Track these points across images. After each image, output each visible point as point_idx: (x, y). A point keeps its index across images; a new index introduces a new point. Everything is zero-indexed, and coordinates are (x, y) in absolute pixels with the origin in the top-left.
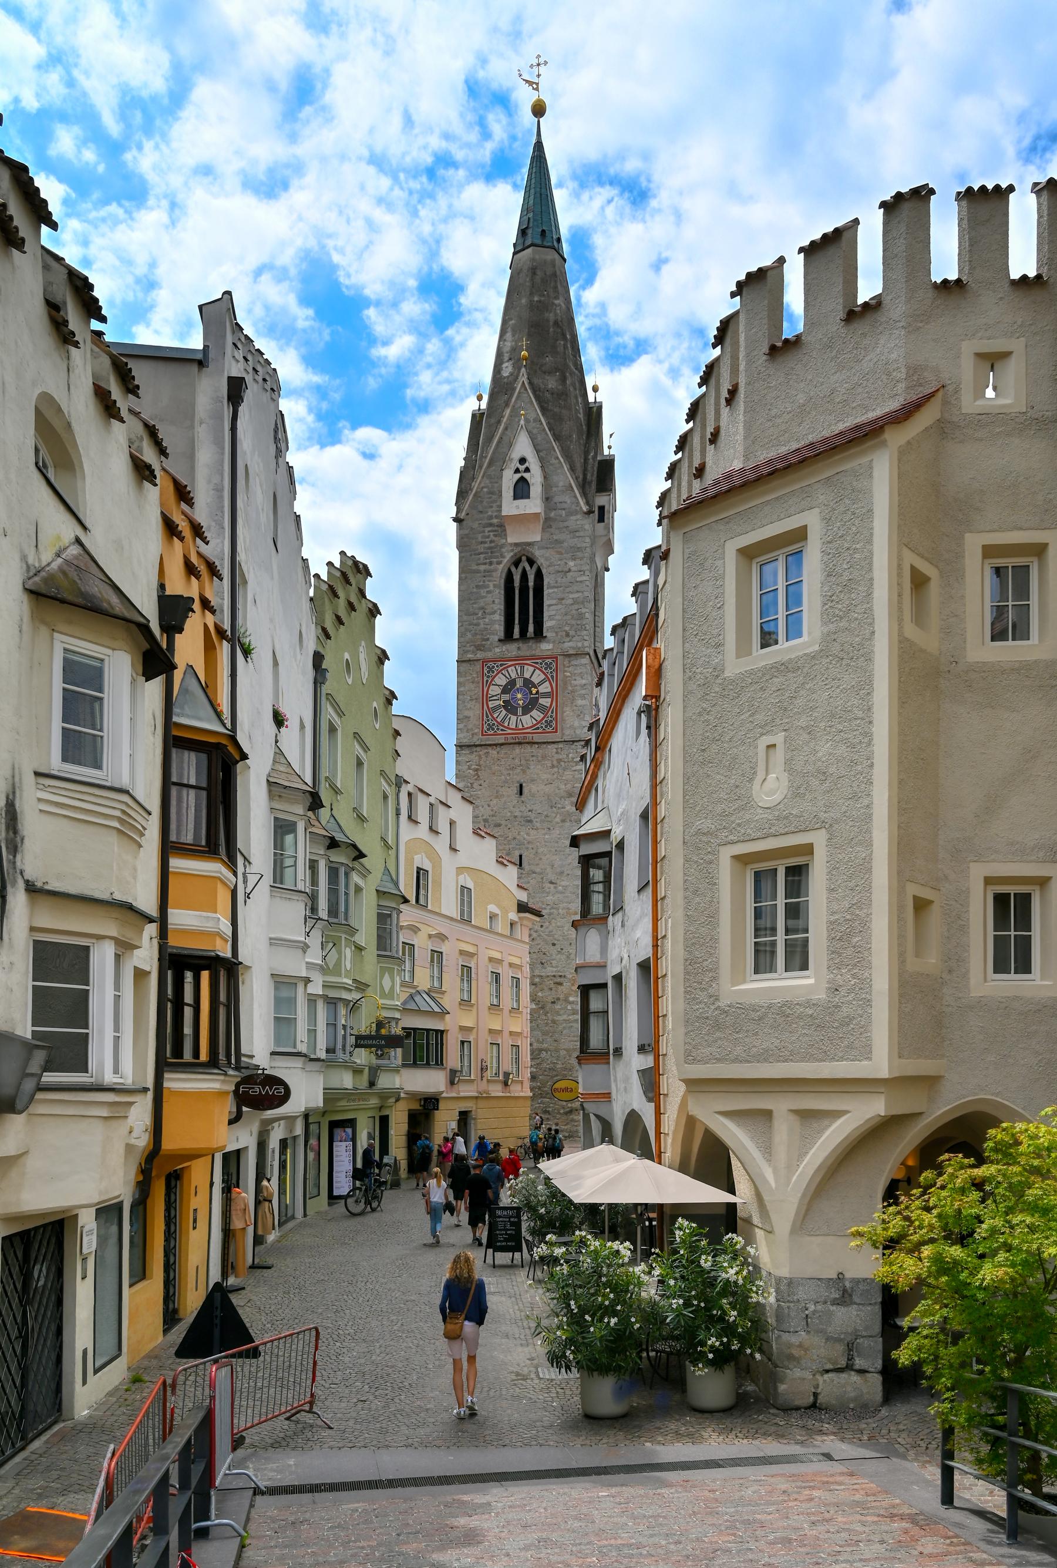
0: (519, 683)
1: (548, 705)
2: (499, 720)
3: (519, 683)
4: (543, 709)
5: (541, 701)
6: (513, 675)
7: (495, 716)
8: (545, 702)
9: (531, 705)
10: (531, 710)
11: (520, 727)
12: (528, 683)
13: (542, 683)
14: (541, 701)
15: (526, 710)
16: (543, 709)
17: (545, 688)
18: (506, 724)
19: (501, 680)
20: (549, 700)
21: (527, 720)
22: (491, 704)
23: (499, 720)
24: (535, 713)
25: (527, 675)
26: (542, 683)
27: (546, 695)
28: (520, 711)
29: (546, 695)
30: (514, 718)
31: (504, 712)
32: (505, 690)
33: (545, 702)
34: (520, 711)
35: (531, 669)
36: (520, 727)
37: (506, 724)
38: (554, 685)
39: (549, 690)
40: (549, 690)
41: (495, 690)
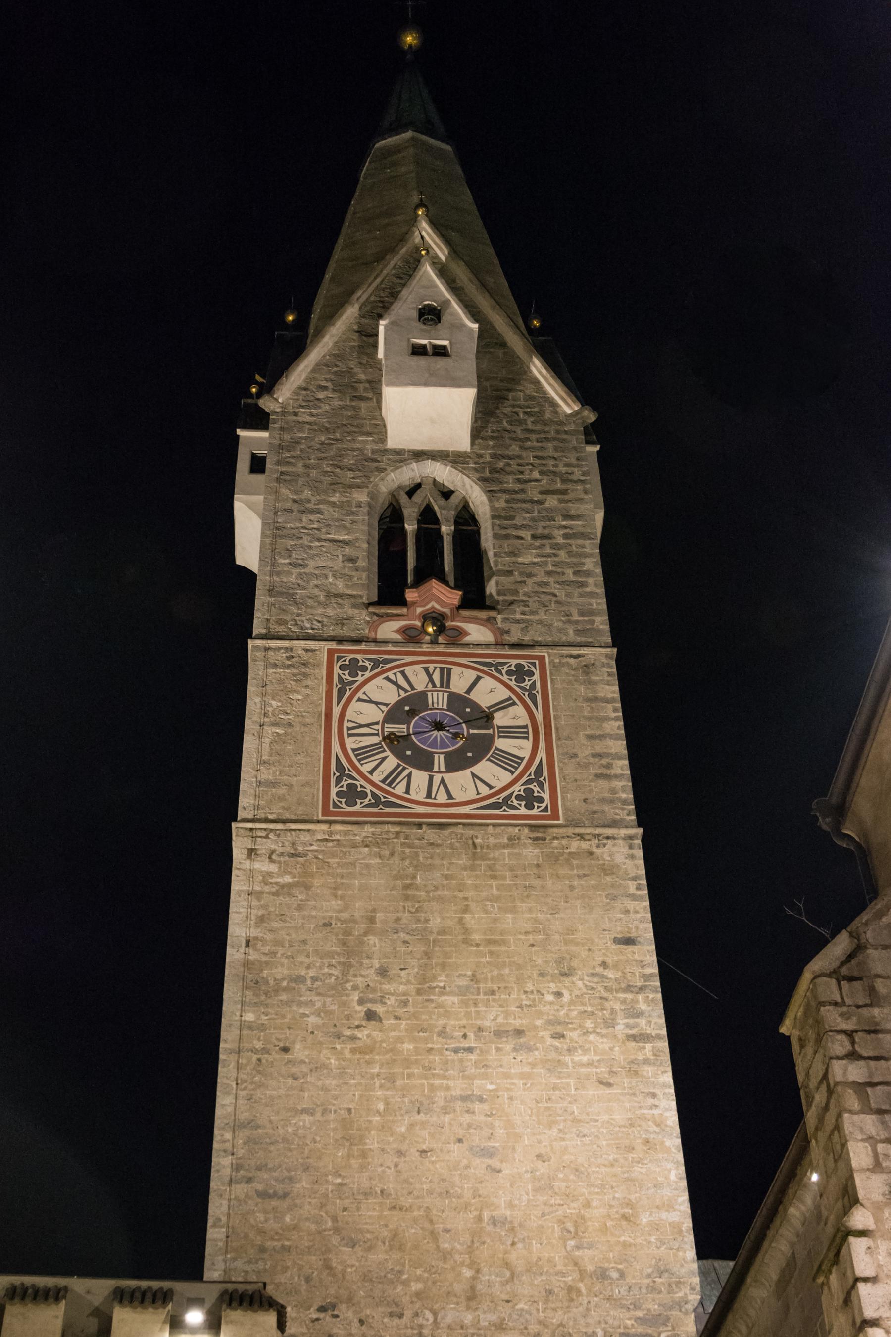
0: (439, 700)
1: (526, 754)
2: (377, 778)
3: (439, 700)
4: (508, 761)
6: (420, 682)
7: (366, 768)
12: (458, 702)
14: (501, 743)
15: (456, 763)
16: (508, 761)
17: (516, 716)
20: (528, 745)
21: (461, 784)
22: (351, 743)
23: (377, 778)
24: (484, 768)
28: (439, 761)
30: (420, 777)
31: (392, 761)
32: (394, 714)
34: (439, 761)
35: (472, 675)
36: (442, 798)
37: (400, 790)
40: (524, 720)
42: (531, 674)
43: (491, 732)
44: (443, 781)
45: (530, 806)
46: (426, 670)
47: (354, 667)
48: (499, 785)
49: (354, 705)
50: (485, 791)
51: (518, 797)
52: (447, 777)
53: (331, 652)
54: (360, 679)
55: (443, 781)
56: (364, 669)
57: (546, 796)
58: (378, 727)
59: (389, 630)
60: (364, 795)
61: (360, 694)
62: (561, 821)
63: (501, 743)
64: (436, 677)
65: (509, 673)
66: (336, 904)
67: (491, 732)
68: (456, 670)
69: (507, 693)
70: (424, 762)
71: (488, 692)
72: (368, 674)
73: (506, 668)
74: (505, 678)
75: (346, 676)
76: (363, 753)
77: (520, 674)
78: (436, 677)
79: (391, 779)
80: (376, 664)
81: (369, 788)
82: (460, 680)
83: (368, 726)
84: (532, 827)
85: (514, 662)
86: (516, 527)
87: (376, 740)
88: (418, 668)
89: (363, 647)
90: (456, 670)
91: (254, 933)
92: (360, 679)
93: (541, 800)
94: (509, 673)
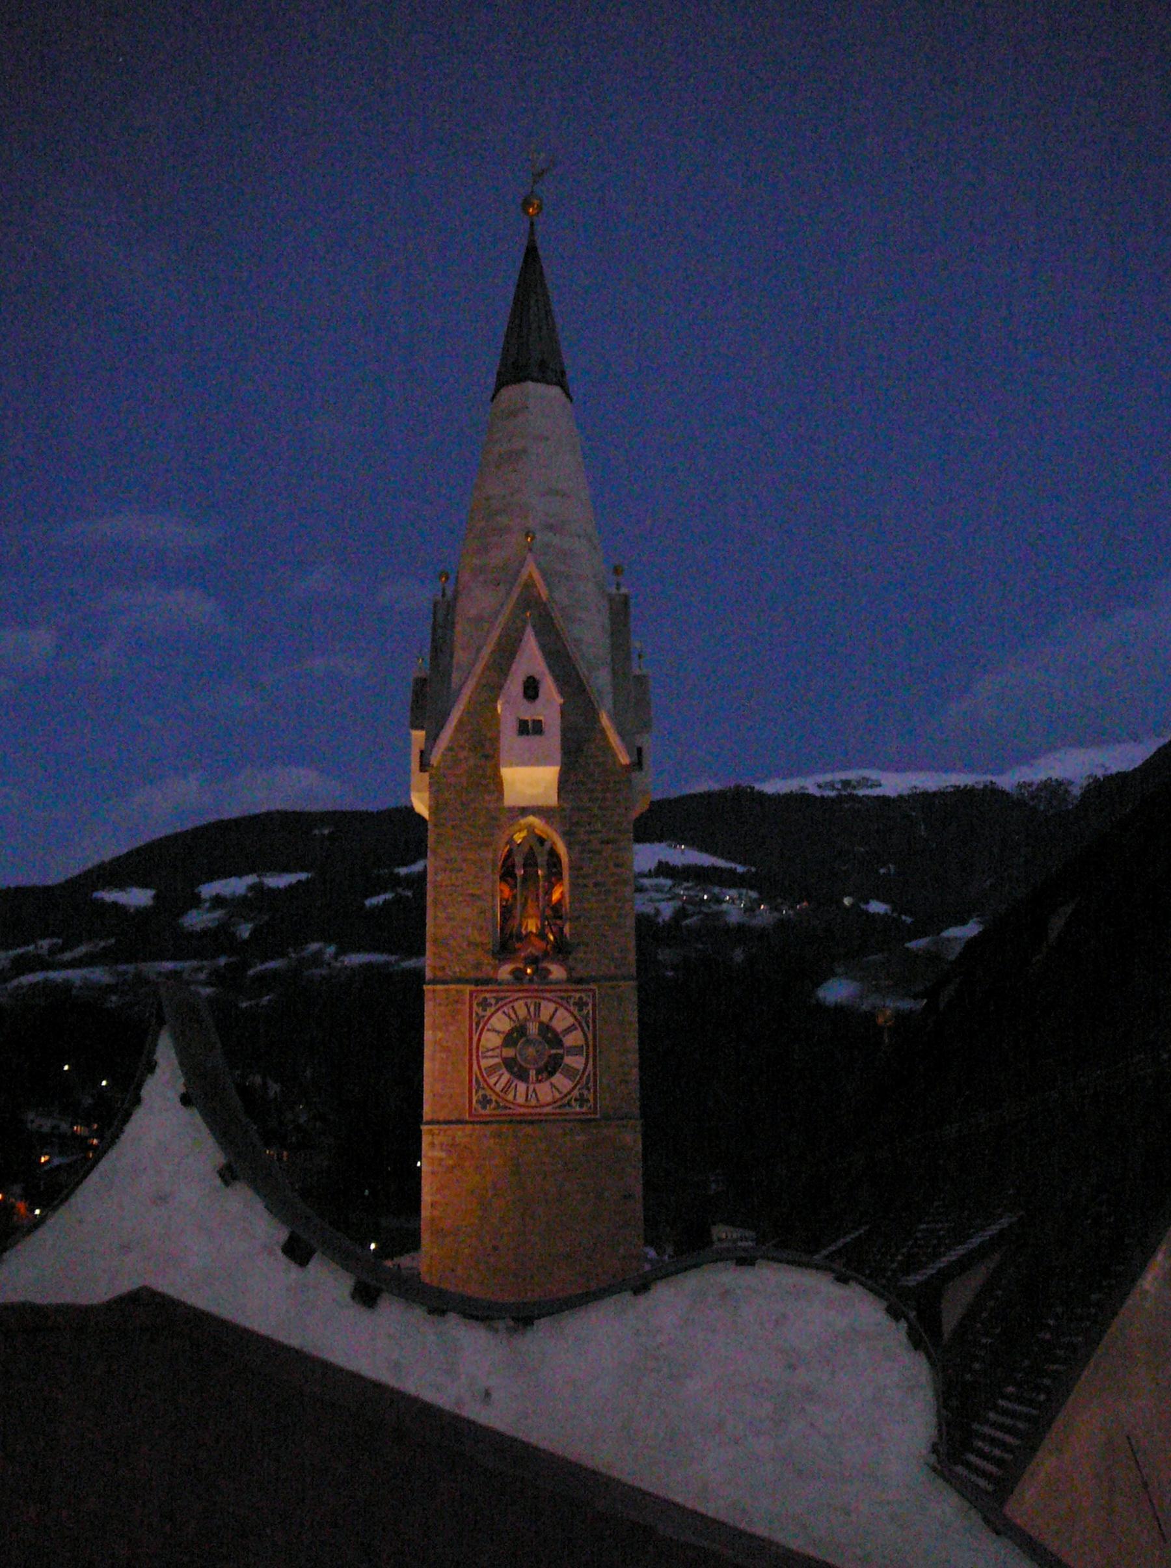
0: (533, 1029)
1: (581, 1067)
3: (533, 1029)
4: (570, 1073)
5: (568, 1060)
7: (492, 1081)
8: (575, 1062)
9: (552, 1067)
10: (551, 1074)
11: (533, 1102)
12: (545, 1028)
13: (569, 1030)
16: (570, 1073)
18: (510, 1097)
19: (501, 1022)
21: (545, 1092)
22: (485, 1063)
23: (498, 1088)
24: (560, 1080)
25: (544, 1017)
26: (569, 1030)
27: (575, 1051)
28: (532, 1073)
29: (575, 1051)
30: (522, 1087)
31: (506, 1076)
32: (510, 1039)
33: (575, 1062)
34: (532, 1073)
35: (552, 1006)
37: (510, 1097)
38: (590, 1037)
39: (581, 1042)
40: (581, 1042)
41: (491, 1040)
42: (586, 1004)
43: (560, 1051)
44: (534, 1090)
45: (581, 1106)
46: (526, 1004)
47: (484, 1004)
48: (565, 1091)
49: (486, 1034)
50: (558, 1095)
51: (576, 1100)
52: (538, 1086)
53: (471, 994)
54: (488, 1013)
55: (534, 1090)
56: (491, 1005)
57: (591, 1097)
58: (498, 1051)
59: (505, 972)
60: (490, 1102)
61: (488, 1026)
62: (598, 1116)
63: (568, 1060)
64: (532, 1009)
65: (575, 1004)
66: (478, 1178)
67: (560, 1051)
68: (544, 1003)
69: (571, 1020)
70: (522, 1075)
71: (562, 1020)
72: (493, 1009)
73: (572, 1001)
74: (572, 1008)
75: (480, 1011)
76: (492, 1070)
77: (581, 1004)
78: (532, 1009)
79: (505, 1090)
80: (498, 1000)
81: (494, 1098)
82: (547, 1009)
83: (493, 1050)
84: (580, 1121)
85: (578, 995)
86: (584, 877)
87: (498, 1060)
88: (521, 1002)
89: (490, 987)
90: (544, 1003)
91: (438, 1197)
92: (488, 1013)
93: (588, 1101)
94: (575, 1004)
